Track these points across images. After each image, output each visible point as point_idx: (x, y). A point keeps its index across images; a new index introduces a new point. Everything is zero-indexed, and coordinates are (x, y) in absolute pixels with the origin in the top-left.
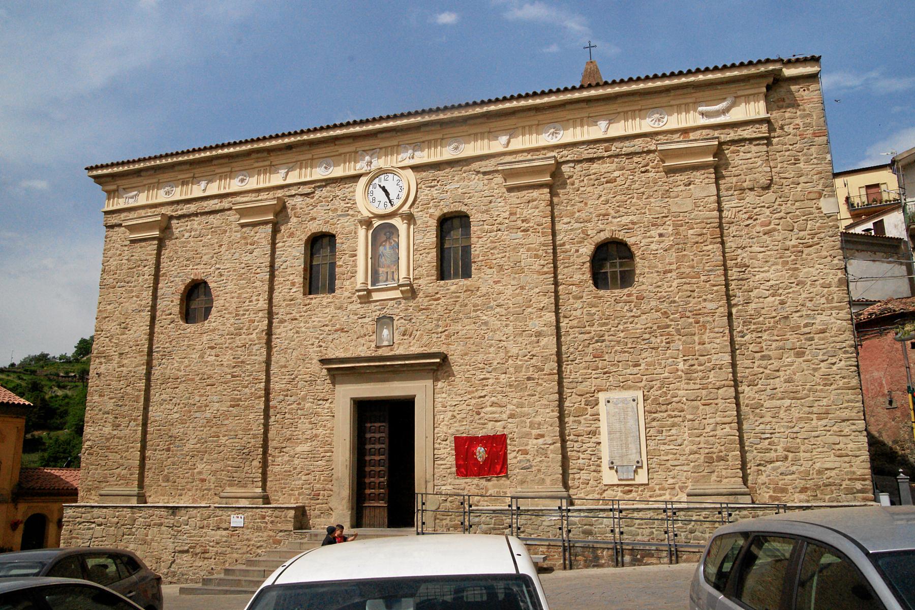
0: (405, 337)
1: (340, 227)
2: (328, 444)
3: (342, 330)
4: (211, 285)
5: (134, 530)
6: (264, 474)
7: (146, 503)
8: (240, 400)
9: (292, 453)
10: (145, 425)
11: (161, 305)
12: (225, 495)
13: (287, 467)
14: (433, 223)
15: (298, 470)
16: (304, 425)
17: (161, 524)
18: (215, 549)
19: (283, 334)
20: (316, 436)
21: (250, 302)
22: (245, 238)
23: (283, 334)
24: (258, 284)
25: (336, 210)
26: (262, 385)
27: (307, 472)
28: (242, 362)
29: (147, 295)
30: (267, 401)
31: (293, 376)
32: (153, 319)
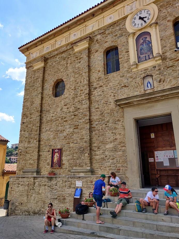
0: (161, 83)
1: (119, 42)
2: (123, 144)
3: (125, 86)
4: (64, 80)
5: (35, 188)
6: (91, 159)
7: (40, 175)
8: (78, 125)
9: (104, 149)
10: (39, 141)
11: (46, 92)
12: (73, 171)
13: (102, 156)
14: (170, 24)
15: (108, 157)
16: (109, 134)
17: (45, 185)
18: (69, 198)
19: (96, 94)
20: (116, 139)
21: (81, 82)
22: (77, 57)
23: (96, 94)
24: (84, 74)
25: (116, 35)
26: (88, 118)
27: (112, 158)
28: (79, 109)
29: (40, 89)
30: (91, 124)
31: (102, 112)
32: (42, 98)
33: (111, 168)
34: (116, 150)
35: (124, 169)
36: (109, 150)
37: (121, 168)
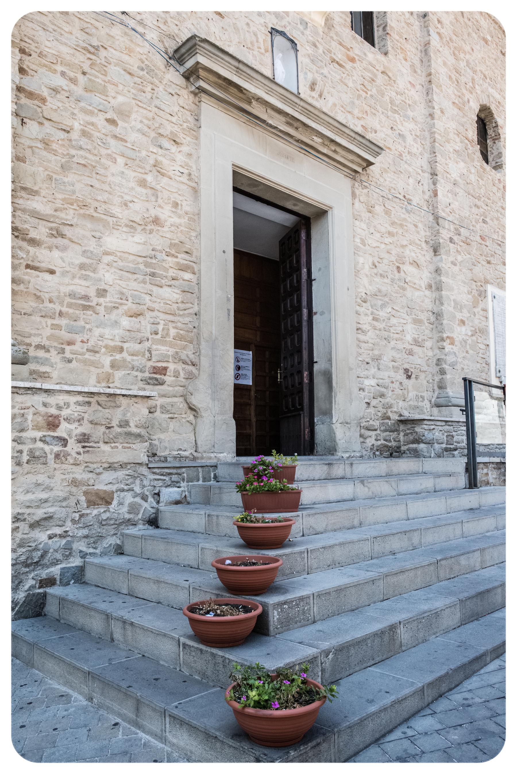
33: (124, 360)
34: (153, 275)
35: (181, 371)
36: (121, 264)
37: (172, 367)
